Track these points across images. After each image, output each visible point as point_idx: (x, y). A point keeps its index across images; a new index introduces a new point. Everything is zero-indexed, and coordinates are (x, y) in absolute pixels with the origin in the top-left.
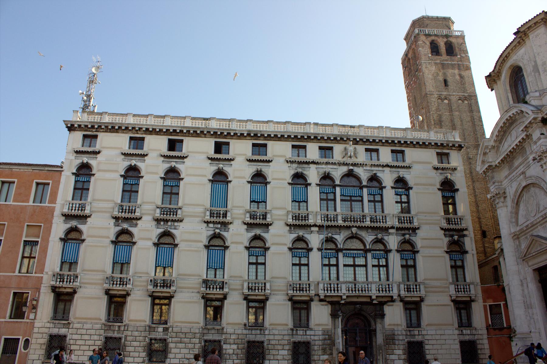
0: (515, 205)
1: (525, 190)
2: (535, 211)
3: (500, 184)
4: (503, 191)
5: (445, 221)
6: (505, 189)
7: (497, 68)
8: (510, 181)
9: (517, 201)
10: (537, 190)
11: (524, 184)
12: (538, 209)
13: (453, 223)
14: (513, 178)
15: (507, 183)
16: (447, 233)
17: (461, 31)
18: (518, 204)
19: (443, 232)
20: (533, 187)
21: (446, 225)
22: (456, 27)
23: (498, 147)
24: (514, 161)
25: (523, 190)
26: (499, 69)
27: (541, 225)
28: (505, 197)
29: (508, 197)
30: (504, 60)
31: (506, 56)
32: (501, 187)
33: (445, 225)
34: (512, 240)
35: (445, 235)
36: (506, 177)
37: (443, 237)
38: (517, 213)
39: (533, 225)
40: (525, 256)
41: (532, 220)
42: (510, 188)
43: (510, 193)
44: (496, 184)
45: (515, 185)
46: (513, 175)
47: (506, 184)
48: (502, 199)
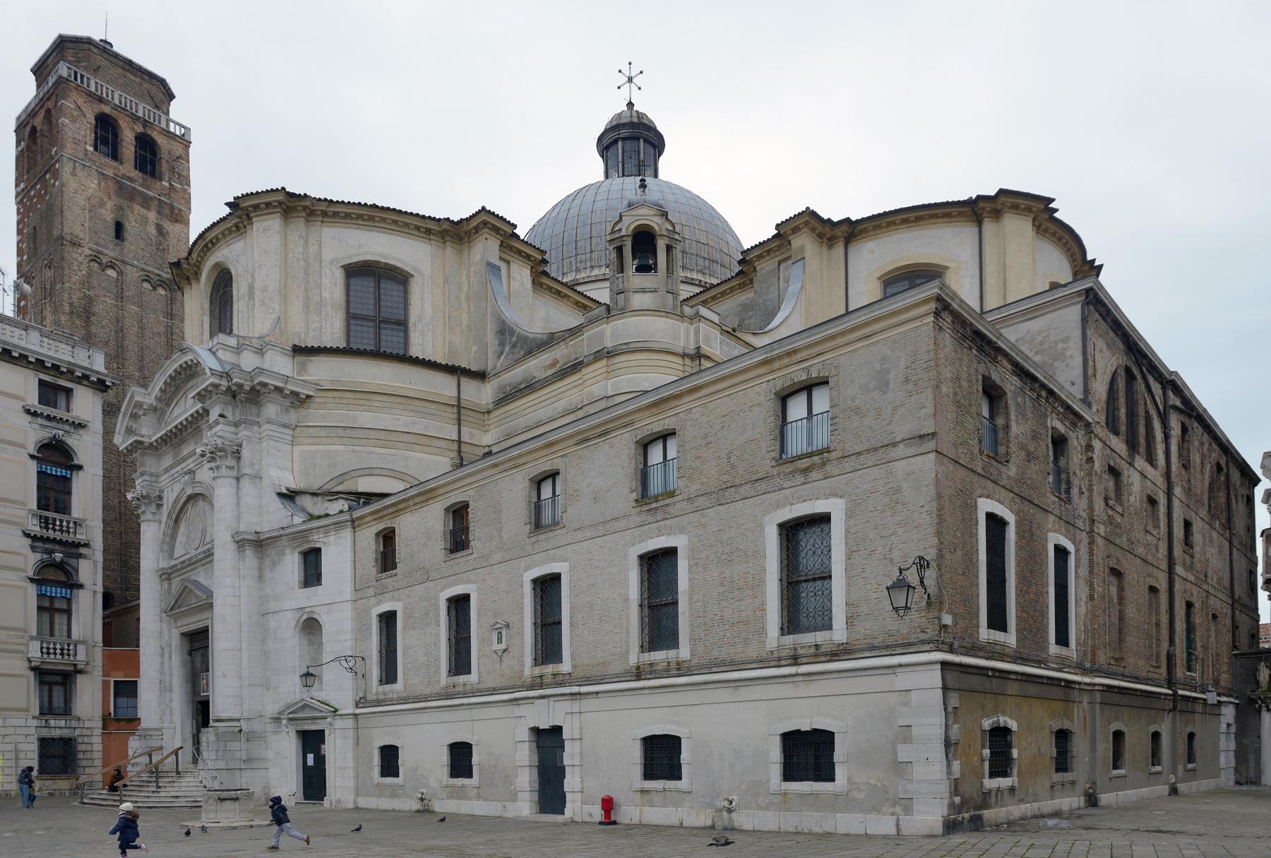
0: (172, 523)
1: (192, 502)
3: (154, 479)
4: (157, 493)
5: (36, 521)
6: (162, 491)
8: (171, 478)
11: (189, 491)
13: (57, 528)
16: (40, 544)
17: (184, 127)
18: (177, 521)
19: (29, 541)
20: (203, 500)
21: (38, 529)
22: (176, 110)
27: (203, 565)
32: (155, 484)
33: (35, 528)
35: (32, 547)
37: (29, 551)
44: (147, 478)
45: (177, 488)
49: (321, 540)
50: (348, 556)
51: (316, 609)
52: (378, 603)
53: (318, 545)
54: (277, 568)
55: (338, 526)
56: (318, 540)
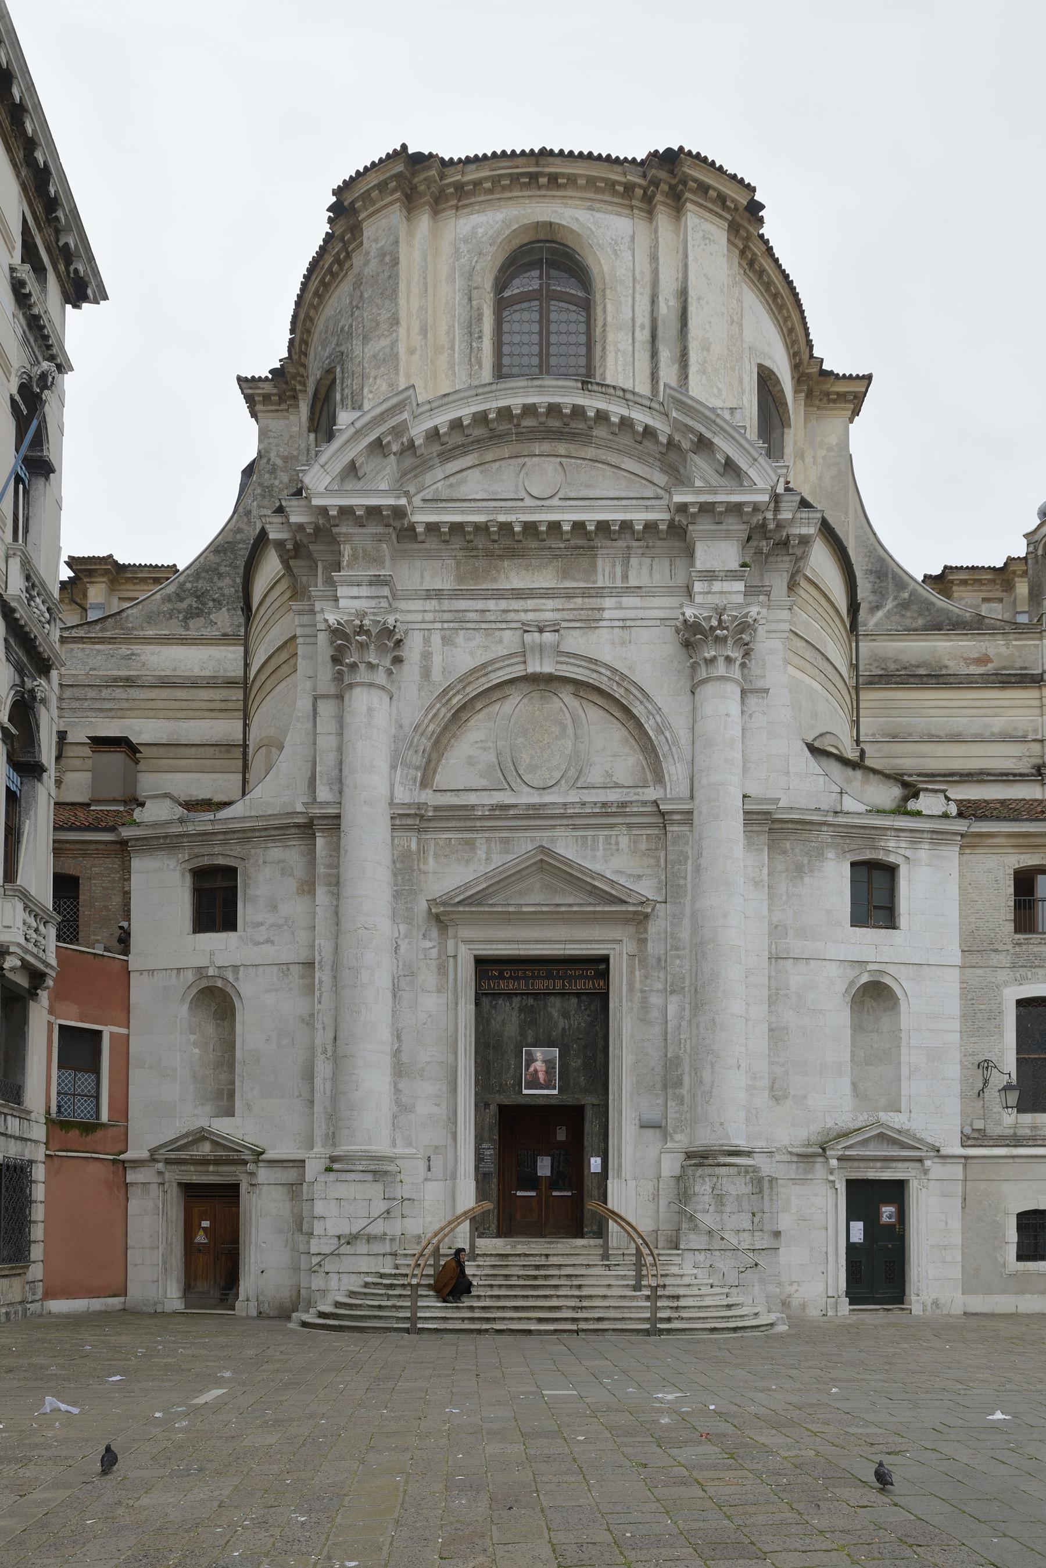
0: (446, 714)
1: (525, 687)
2: (557, 775)
7: (473, 174)
8: (447, 616)
9: (463, 708)
10: (593, 716)
12: (573, 773)
14: (472, 616)
15: (429, 617)
18: (459, 716)
23: (423, 466)
24: (506, 563)
25: (512, 682)
26: (477, 183)
27: (575, 827)
28: (398, 660)
29: (411, 670)
30: (534, 177)
31: (553, 179)
34: (389, 822)
36: (437, 594)
38: (440, 744)
39: (536, 814)
40: (459, 903)
41: (527, 797)
42: (436, 639)
43: (426, 656)
46: (480, 605)
47: (419, 617)
48: (387, 662)
49: (902, 851)
50: (953, 891)
51: (890, 969)
52: (1021, 981)
53: (892, 859)
54: (807, 880)
55: (938, 837)
56: (893, 850)
